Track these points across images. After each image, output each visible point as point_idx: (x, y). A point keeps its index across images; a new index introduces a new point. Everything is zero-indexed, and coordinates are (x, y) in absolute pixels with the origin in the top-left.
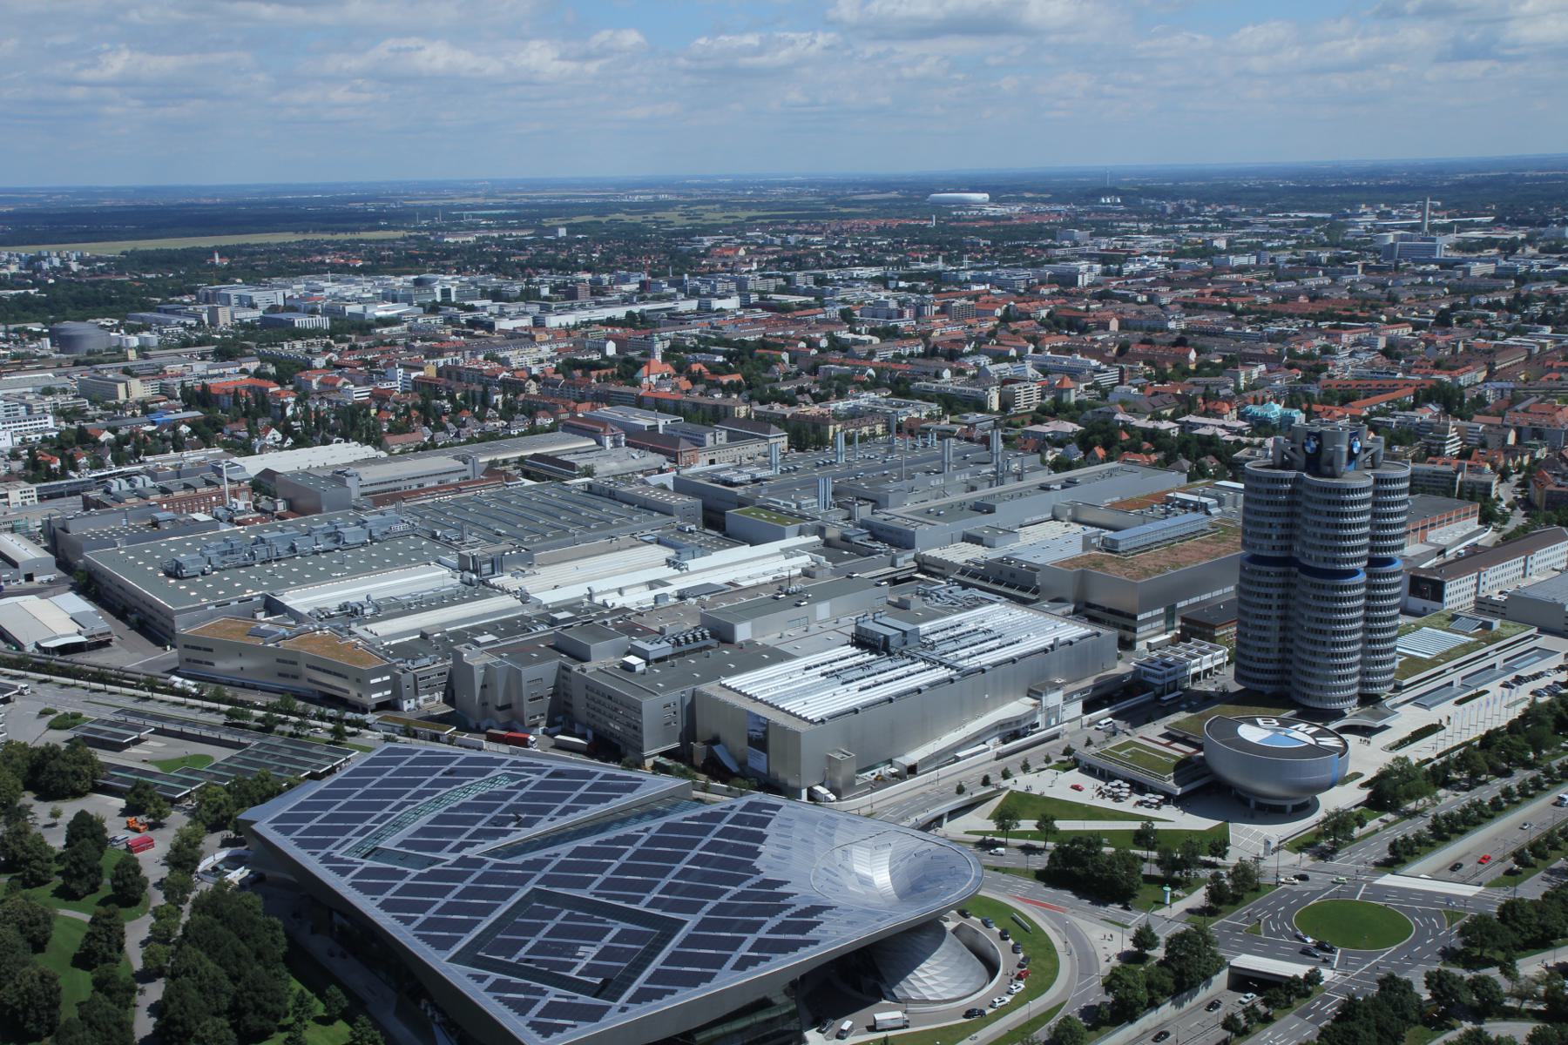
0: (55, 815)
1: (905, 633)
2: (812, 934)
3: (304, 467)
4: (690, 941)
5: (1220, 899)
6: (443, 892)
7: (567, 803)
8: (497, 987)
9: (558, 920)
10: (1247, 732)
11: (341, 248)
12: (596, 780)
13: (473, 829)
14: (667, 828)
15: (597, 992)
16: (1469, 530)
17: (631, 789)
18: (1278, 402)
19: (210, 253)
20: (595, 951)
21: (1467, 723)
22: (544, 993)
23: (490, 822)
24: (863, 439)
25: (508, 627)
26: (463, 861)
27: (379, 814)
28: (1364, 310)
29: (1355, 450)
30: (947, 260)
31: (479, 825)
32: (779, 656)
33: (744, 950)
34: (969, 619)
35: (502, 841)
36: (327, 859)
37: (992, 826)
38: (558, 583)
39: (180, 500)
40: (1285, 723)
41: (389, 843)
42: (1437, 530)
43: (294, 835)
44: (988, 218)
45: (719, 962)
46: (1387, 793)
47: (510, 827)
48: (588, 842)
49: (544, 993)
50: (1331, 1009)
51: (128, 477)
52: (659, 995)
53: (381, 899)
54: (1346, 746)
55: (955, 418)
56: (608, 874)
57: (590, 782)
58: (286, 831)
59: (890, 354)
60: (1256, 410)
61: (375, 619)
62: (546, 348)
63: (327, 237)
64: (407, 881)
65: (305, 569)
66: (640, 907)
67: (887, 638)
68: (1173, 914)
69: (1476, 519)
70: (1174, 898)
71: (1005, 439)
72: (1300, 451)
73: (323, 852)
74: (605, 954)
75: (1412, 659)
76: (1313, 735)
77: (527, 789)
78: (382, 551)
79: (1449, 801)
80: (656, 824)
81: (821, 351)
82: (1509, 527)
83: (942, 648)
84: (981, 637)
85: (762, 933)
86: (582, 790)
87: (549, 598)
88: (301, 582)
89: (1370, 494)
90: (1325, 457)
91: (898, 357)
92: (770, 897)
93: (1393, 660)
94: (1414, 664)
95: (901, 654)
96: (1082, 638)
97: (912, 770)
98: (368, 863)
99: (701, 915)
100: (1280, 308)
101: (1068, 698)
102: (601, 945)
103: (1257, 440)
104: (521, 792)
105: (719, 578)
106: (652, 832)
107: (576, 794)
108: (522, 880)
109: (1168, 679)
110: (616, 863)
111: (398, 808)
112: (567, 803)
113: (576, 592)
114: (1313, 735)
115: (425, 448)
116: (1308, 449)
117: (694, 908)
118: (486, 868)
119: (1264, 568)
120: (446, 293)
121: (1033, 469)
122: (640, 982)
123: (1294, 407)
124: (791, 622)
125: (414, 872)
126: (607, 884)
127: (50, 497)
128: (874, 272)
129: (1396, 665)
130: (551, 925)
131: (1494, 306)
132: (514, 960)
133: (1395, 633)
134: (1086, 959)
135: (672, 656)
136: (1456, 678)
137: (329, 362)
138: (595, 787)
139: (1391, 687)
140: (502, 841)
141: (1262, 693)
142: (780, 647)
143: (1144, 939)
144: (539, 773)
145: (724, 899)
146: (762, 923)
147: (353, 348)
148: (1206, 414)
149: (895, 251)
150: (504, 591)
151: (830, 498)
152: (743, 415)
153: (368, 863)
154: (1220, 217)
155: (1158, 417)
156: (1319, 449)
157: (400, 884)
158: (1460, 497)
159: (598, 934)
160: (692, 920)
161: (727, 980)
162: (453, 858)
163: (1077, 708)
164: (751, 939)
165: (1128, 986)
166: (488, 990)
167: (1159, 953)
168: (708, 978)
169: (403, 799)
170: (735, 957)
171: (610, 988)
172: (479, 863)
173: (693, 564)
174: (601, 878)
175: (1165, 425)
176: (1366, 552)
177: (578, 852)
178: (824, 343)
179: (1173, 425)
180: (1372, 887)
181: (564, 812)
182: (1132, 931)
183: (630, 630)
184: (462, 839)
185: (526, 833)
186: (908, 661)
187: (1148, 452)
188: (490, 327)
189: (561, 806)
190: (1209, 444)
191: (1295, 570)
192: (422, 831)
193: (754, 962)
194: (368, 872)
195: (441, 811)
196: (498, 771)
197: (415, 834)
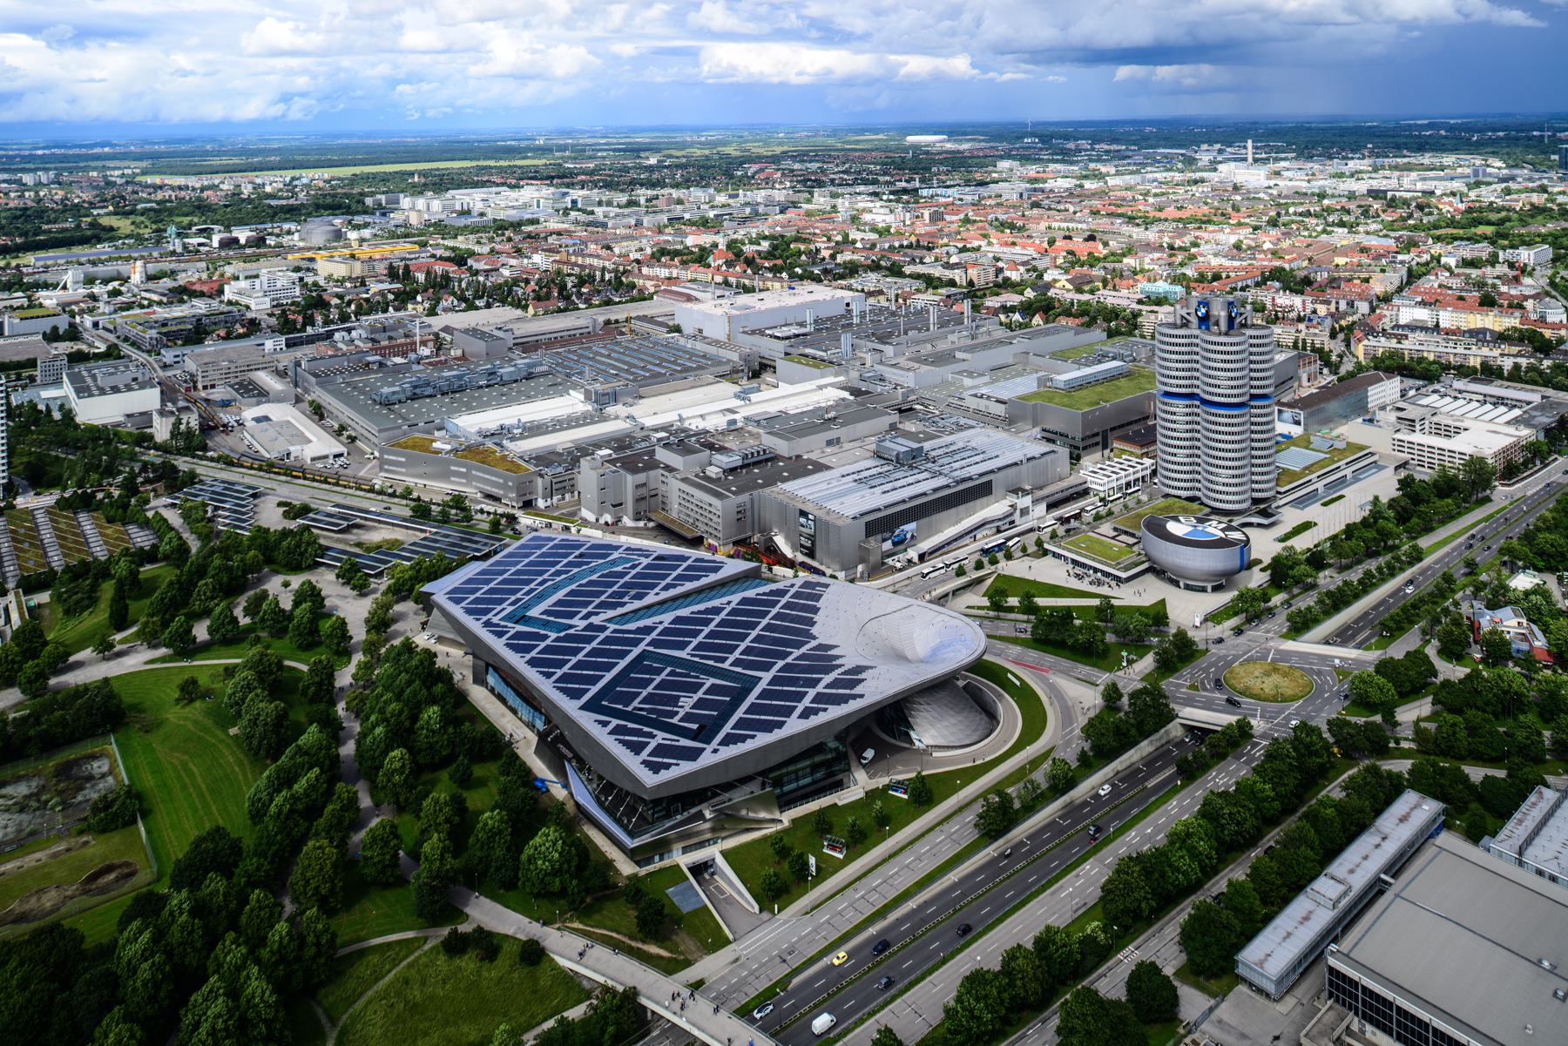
0: (286, 585)
2: (858, 690)
3: (473, 325)
4: (765, 694)
5: (1167, 665)
6: (575, 651)
7: (668, 580)
8: (617, 731)
9: (663, 676)
11: (501, 170)
12: (689, 562)
13: (598, 601)
14: (744, 601)
15: (693, 736)
17: (716, 570)
19: (412, 174)
20: (691, 702)
21: (1330, 521)
22: (653, 737)
23: (610, 596)
25: (620, 443)
26: (590, 627)
27: (527, 588)
28: (1217, 217)
30: (922, 181)
31: (603, 598)
32: (820, 467)
33: (806, 702)
35: (620, 611)
36: (488, 624)
37: (985, 602)
38: (657, 411)
39: (385, 348)
41: (535, 612)
43: (463, 604)
44: (947, 152)
45: (788, 712)
46: (1282, 572)
47: (626, 599)
48: (685, 612)
49: (653, 737)
50: (1259, 753)
51: (349, 330)
52: (743, 739)
53: (528, 657)
56: (700, 638)
57: (685, 565)
58: (457, 601)
59: (887, 246)
61: (522, 437)
63: (492, 163)
64: (548, 642)
65: (474, 398)
66: (726, 665)
68: (1136, 672)
70: (1130, 662)
73: (485, 618)
74: (700, 704)
77: (638, 569)
78: (527, 383)
79: (1328, 579)
80: (736, 598)
82: (1343, 371)
85: (820, 688)
86: (679, 571)
87: (649, 422)
88: (469, 409)
91: (892, 248)
92: (823, 660)
97: (922, 558)
98: (520, 628)
99: (773, 672)
100: (1158, 214)
102: (696, 697)
104: (634, 572)
105: (773, 408)
106: (733, 605)
107: (675, 574)
108: (636, 643)
110: (707, 630)
111: (541, 584)
112: (668, 580)
113: (669, 417)
115: (560, 311)
117: (766, 667)
118: (607, 633)
120: (574, 202)
122: (727, 729)
124: (830, 443)
125: (553, 635)
126: (699, 647)
127: (295, 345)
128: (871, 188)
130: (658, 679)
131: (1308, 214)
132: (630, 709)
134: (1067, 715)
135: (742, 467)
137: (492, 250)
138: (688, 568)
140: (620, 611)
143: (1112, 694)
144: (647, 556)
145: (789, 660)
146: (820, 680)
147: (510, 240)
149: (885, 174)
150: (617, 418)
153: (520, 628)
154: (1107, 152)
157: (543, 645)
159: (694, 688)
160: (766, 677)
161: (794, 725)
162: (584, 623)
164: (812, 693)
166: (611, 733)
168: (780, 725)
169: (545, 576)
170: (800, 707)
171: (705, 732)
172: (602, 629)
173: (754, 397)
174: (695, 642)
175: (1085, 297)
177: (678, 620)
178: (839, 238)
180: (1278, 651)
181: (666, 588)
182: (1102, 688)
183: (711, 447)
184: (590, 608)
185: (637, 604)
188: (604, 225)
189: (663, 583)
192: (559, 603)
193: (815, 712)
194: (518, 635)
195: (573, 587)
196: (616, 555)
197: (554, 605)
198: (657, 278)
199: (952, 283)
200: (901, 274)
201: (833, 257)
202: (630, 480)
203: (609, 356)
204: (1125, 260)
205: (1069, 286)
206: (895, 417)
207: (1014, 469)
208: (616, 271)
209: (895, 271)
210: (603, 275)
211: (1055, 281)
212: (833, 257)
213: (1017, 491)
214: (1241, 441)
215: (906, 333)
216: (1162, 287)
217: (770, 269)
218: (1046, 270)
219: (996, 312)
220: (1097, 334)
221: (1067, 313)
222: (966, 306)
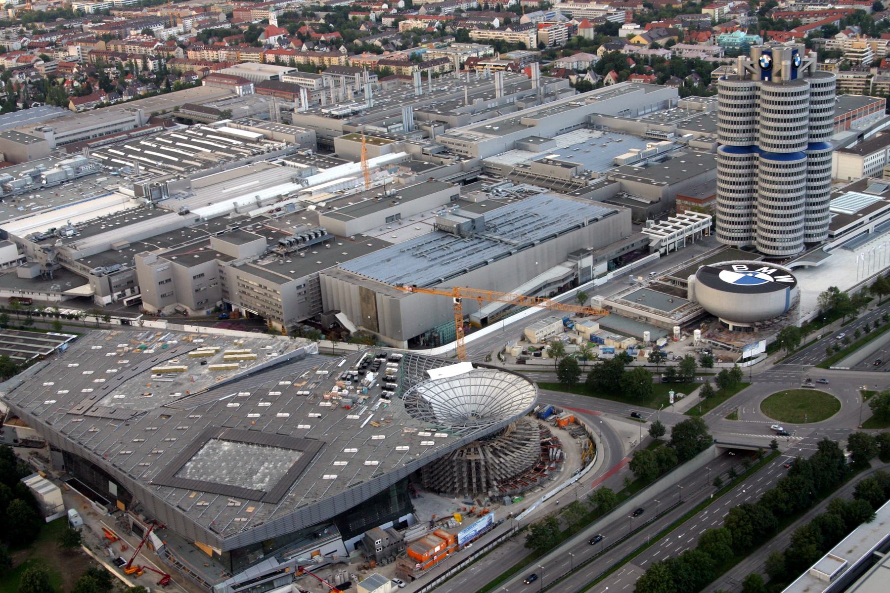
1: (473, 221)
5: (710, 399)
10: (726, 276)
16: (880, 119)
18: (743, 31)
24: (435, 76)
29: (797, 64)
34: (521, 206)
40: (753, 268)
42: (858, 120)
54: (796, 282)
55: (503, 56)
60: (725, 38)
62: (189, 22)
67: (459, 226)
69: (884, 110)
70: (676, 399)
71: (543, 70)
72: (756, 66)
75: (842, 215)
76: (772, 275)
81: (399, 9)
83: (501, 230)
84: (530, 220)
89: (807, 96)
90: (775, 69)
93: (827, 217)
94: (841, 220)
95: (471, 236)
96: (605, 216)
101: (596, 262)
103: (728, 60)
109: (669, 242)
114: (772, 275)
115: (102, 105)
116: (763, 65)
119: (734, 155)
121: (563, 91)
123: (754, 34)
129: (830, 221)
133: (828, 197)
136: (871, 227)
139: (826, 236)
141: (735, 247)
142: (382, 238)
143: (656, 430)
148: (692, 43)
151: (412, 123)
152: (343, 64)
155: (655, 46)
156: (771, 62)
158: (874, 94)
163: (603, 267)
165: (645, 463)
167: (667, 437)
175: (660, 52)
176: (805, 139)
179: (667, 51)
186: (476, 241)
187: (649, 74)
190: (694, 65)
191: (756, 155)
198: (203, 61)
199: (522, 46)
200: (469, 41)
201: (395, 25)
202: (187, 273)
203: (157, 150)
204: (704, 11)
205: (643, 41)
206: (456, 189)
207: (579, 231)
208: (158, 57)
209: (463, 37)
210: (145, 68)
211: (631, 36)
212: (395, 25)
213: (581, 253)
214: (798, 190)
215: (470, 102)
216: (740, 36)
217: (325, 44)
218: (620, 25)
219: (565, 73)
220: (670, 92)
221: (639, 71)
222: (535, 68)
